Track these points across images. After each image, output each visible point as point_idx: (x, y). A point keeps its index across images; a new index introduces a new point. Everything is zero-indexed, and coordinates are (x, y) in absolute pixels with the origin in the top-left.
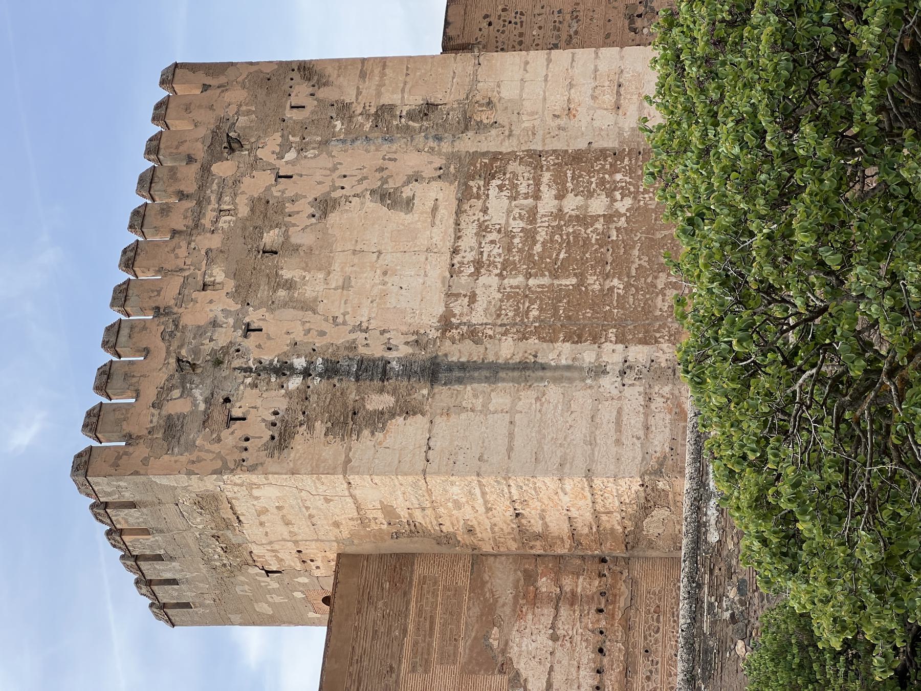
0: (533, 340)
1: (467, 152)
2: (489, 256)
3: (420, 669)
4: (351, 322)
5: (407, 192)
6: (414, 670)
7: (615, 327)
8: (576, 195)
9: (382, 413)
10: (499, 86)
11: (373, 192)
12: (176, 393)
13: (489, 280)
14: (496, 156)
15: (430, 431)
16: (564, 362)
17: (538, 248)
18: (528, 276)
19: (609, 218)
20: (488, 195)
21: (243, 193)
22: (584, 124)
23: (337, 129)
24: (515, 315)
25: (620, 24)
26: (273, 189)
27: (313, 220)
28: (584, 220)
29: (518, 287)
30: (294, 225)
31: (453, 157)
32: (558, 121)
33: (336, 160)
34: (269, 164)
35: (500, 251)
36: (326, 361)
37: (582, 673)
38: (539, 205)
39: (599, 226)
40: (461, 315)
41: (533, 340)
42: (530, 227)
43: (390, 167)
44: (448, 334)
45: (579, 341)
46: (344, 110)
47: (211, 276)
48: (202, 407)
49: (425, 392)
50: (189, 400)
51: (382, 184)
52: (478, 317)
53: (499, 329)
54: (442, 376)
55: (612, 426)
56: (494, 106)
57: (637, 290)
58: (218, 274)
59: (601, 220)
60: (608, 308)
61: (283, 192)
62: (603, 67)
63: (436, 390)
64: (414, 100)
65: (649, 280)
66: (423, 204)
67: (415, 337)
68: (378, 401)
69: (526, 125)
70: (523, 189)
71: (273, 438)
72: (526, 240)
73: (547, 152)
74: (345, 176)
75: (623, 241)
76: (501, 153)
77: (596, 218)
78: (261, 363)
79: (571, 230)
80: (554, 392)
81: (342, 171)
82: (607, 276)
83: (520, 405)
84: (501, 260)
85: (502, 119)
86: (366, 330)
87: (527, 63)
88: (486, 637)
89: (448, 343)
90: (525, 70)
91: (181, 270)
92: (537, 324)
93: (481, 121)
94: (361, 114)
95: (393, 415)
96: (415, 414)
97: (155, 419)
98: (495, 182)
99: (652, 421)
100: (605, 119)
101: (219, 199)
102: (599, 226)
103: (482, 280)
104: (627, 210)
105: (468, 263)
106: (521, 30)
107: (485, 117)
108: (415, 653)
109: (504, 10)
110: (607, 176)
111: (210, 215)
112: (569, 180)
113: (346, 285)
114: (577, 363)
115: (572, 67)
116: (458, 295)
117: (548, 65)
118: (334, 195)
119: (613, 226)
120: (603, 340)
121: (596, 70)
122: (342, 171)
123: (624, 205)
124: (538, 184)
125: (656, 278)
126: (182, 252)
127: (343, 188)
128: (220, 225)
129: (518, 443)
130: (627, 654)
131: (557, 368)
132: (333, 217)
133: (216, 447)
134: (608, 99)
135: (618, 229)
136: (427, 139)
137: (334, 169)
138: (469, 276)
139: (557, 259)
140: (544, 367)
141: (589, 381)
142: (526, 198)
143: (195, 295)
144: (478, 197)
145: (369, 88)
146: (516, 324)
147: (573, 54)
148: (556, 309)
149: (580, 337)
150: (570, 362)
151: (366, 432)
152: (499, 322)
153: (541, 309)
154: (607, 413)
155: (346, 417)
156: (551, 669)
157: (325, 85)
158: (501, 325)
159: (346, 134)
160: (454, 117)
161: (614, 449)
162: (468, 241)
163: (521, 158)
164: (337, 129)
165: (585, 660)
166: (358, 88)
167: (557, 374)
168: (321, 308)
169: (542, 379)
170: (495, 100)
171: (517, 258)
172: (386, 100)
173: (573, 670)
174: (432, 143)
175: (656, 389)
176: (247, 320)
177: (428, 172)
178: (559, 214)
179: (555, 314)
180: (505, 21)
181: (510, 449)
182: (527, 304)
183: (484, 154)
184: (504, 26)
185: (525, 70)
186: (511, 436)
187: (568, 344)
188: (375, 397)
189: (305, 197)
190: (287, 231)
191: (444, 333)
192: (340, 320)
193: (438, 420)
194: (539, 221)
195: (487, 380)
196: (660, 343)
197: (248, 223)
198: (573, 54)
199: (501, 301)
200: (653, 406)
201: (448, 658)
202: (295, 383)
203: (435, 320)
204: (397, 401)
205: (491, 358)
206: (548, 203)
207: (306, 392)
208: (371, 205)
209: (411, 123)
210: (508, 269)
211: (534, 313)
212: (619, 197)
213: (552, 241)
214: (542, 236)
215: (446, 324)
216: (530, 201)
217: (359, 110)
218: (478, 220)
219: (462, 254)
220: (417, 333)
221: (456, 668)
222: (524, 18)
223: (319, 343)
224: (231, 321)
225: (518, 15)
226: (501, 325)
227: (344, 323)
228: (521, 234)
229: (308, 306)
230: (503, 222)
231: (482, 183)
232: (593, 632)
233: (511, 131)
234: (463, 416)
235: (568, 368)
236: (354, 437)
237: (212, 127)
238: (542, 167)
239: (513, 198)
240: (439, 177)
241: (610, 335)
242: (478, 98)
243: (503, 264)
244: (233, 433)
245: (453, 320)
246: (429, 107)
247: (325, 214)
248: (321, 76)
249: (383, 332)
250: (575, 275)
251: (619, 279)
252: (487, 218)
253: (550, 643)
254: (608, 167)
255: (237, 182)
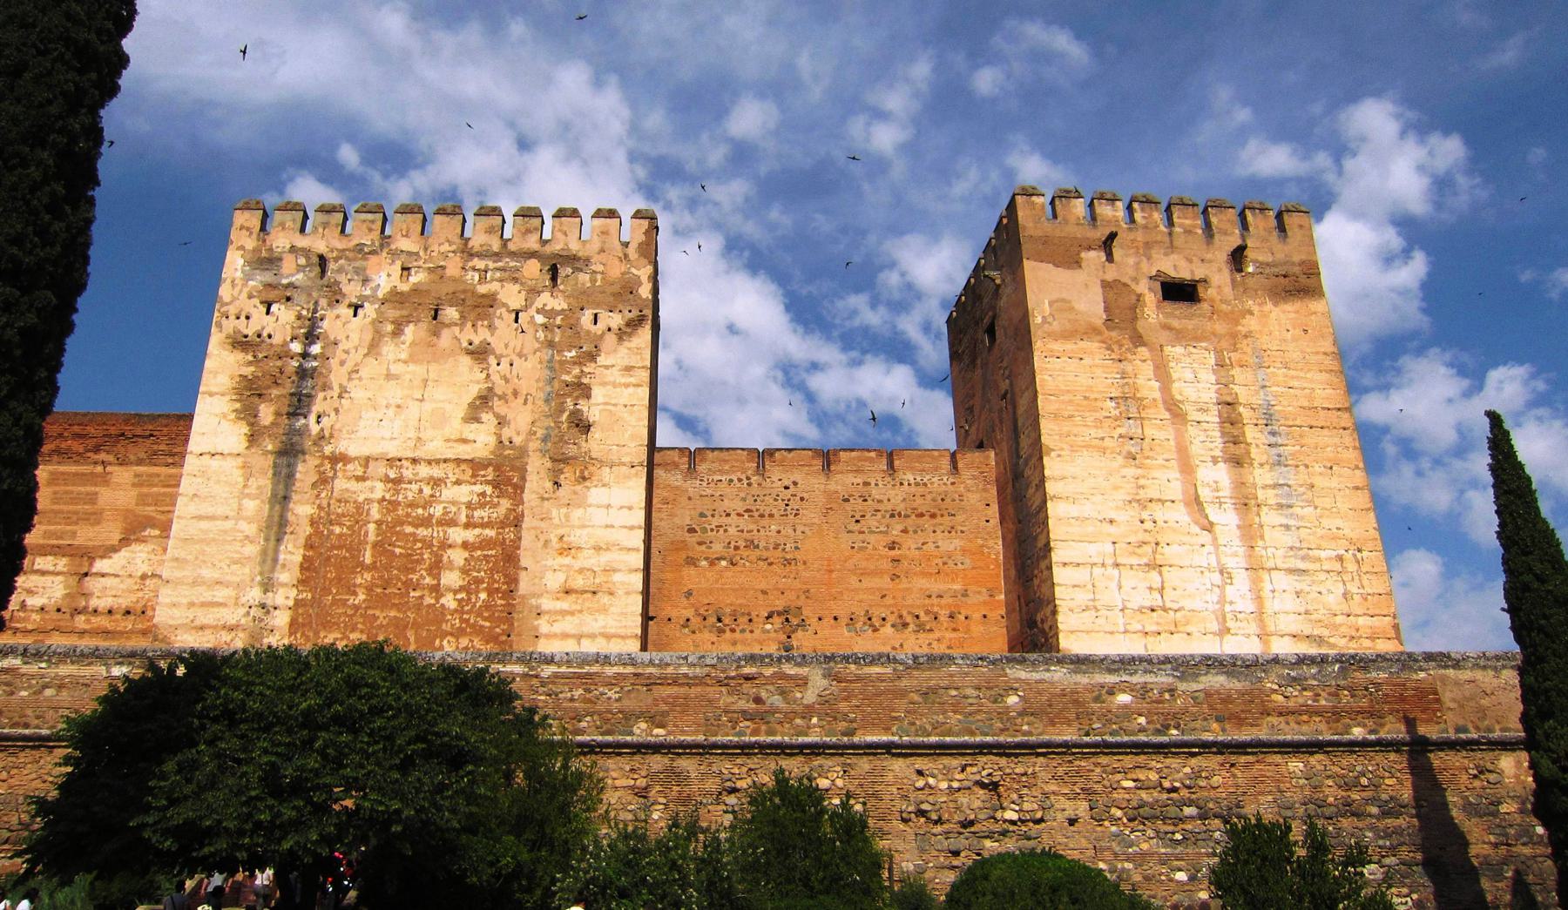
0: (309, 530)
1: (527, 463)
2: (406, 489)
3: (136, 480)
4: (350, 386)
5: (485, 417)
6: (136, 475)
7: (313, 597)
8: (466, 559)
9: (256, 416)
10: (604, 485)
11: (490, 389)
12: (302, 261)
13: (380, 490)
14: (519, 488)
15: (229, 454)
16: (282, 557)
17: (409, 529)
18: (379, 523)
19: (436, 590)
20: (475, 484)
21: (502, 286)
22: (550, 563)
23: (566, 354)
24: (338, 514)
25: (777, 602)
26: (504, 310)
27: (465, 344)
28: (436, 567)
29: (368, 514)
30: (461, 330)
31: (523, 452)
32: (555, 540)
33: (530, 357)
34: (533, 303)
35: (410, 498)
36: (315, 369)
37: (110, 600)
38: (458, 529)
39: (428, 580)
40: (345, 470)
41: (309, 530)
42: (434, 521)
43: (518, 400)
44: (326, 462)
45: (302, 568)
46: (592, 357)
47: (416, 272)
48: (285, 281)
49: (270, 447)
50: (294, 271)
51: (497, 395)
52: (340, 484)
53: (325, 503)
54: (284, 460)
55: (210, 599)
56: (579, 483)
57: (351, 616)
58: (417, 278)
59: (435, 582)
60: (334, 591)
61: (499, 318)
62: (617, 577)
63: (269, 456)
64: (593, 410)
65: (360, 626)
66: (471, 431)
67: (327, 435)
68: (266, 414)
69: (554, 513)
70: (477, 514)
71: (246, 336)
72: (419, 518)
73: (520, 532)
74: (511, 365)
75: (407, 602)
76: (523, 492)
77: (437, 577)
78: (322, 320)
79: (425, 556)
80: (252, 550)
81: (517, 362)
82: (369, 589)
83: (243, 525)
84: (400, 499)
85: (561, 492)
86: (340, 397)
87: (630, 508)
88: (153, 526)
89: (317, 462)
90: (621, 508)
91: (426, 249)
92: (325, 532)
93: (562, 473)
94: (582, 371)
95: (251, 425)
96: (249, 441)
97: (279, 250)
98: (489, 489)
99: (208, 632)
100: (554, 581)
101: (498, 269)
102: (428, 580)
103: (380, 486)
104: (443, 605)
105: (401, 473)
106: (777, 516)
107: (568, 475)
108: (151, 475)
109: (802, 499)
110: (485, 585)
111: (480, 264)
112: (486, 553)
113: (389, 376)
114: (279, 567)
115: (621, 549)
116: (366, 466)
117: (626, 527)
118: (492, 360)
119: (426, 592)
120: (300, 588)
121: (615, 571)
122: (517, 362)
123: (449, 601)
124: (483, 526)
125: (362, 632)
126: (446, 247)
127: (498, 364)
128: (470, 273)
129: (204, 525)
130: (122, 633)
131: (276, 551)
132: (466, 360)
133: (244, 295)
134: (579, 582)
135: (422, 597)
136: (547, 429)
137: (520, 355)
138: (386, 474)
139: (395, 546)
140: (279, 540)
141: (259, 578)
142: (467, 516)
143: (398, 265)
144: (474, 476)
145: (615, 375)
146: (329, 515)
147: (637, 550)
148: (340, 547)
149: (308, 569)
150: (281, 562)
151: (238, 405)
152: (332, 502)
153: (341, 535)
154: (221, 594)
155: (256, 389)
156: (117, 576)
157: (620, 339)
158: (329, 505)
159: (560, 361)
160: (571, 450)
161: (185, 601)
162: (424, 471)
163: (514, 510)
164: (566, 354)
165: (120, 600)
166: (613, 366)
167: (270, 552)
168: (371, 360)
169: (267, 539)
170: (587, 483)
171: (400, 512)
172: (598, 393)
173: (114, 593)
174: (540, 433)
175: (241, 635)
176: (366, 304)
177: (507, 433)
178: (445, 545)
179: (333, 547)
180: (789, 500)
181: (200, 518)
182: (348, 523)
183: (523, 479)
184: (783, 500)
185: (621, 508)
186: (212, 518)
187: (300, 559)
188: (272, 409)
189: (492, 335)
190: (456, 325)
191: (328, 457)
192: (354, 376)
193: (240, 460)
194: (440, 529)
195: (274, 495)
196: (290, 636)
197: (469, 294)
198: (637, 550)
199: (355, 502)
200: (224, 633)
201: (142, 500)
202: (296, 347)
203: (342, 450)
204: (265, 427)
205: (295, 497)
206: (457, 535)
207: (286, 357)
208: (474, 390)
209: (567, 413)
210: (390, 507)
211: (337, 530)
212: (459, 596)
213: (415, 541)
214: (422, 532)
215: (338, 459)
216: (463, 519)
217: (586, 370)
218: (447, 478)
219: (411, 467)
220: (332, 436)
221: (132, 506)
222: (792, 517)
223: (334, 362)
224: (368, 292)
225: (794, 512)
226: (329, 505)
227: (350, 379)
228: (426, 514)
229: (373, 348)
230: (443, 498)
231: (490, 478)
232: (145, 606)
233: (548, 499)
234: (241, 479)
235: (275, 560)
236: (234, 397)
237: (580, 254)
238: (503, 528)
239: (469, 506)
240: (501, 442)
241: (305, 594)
242: (591, 468)
243: (394, 501)
244: (255, 306)
245: (340, 465)
246: (582, 426)
247: (470, 353)
248: (630, 335)
249: (337, 411)
250: (375, 562)
251: (364, 601)
252: (449, 485)
253: (139, 574)
254: (496, 586)
255: (515, 280)
